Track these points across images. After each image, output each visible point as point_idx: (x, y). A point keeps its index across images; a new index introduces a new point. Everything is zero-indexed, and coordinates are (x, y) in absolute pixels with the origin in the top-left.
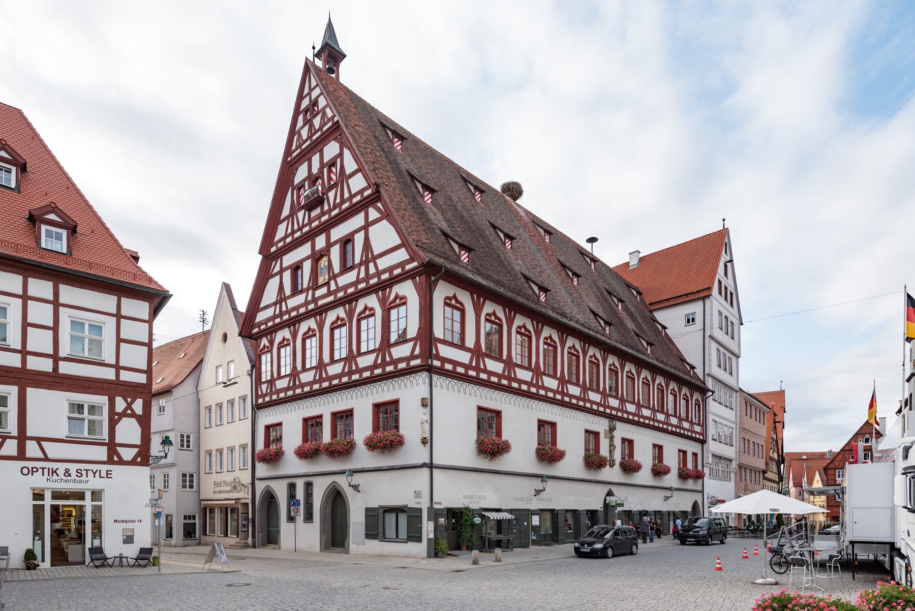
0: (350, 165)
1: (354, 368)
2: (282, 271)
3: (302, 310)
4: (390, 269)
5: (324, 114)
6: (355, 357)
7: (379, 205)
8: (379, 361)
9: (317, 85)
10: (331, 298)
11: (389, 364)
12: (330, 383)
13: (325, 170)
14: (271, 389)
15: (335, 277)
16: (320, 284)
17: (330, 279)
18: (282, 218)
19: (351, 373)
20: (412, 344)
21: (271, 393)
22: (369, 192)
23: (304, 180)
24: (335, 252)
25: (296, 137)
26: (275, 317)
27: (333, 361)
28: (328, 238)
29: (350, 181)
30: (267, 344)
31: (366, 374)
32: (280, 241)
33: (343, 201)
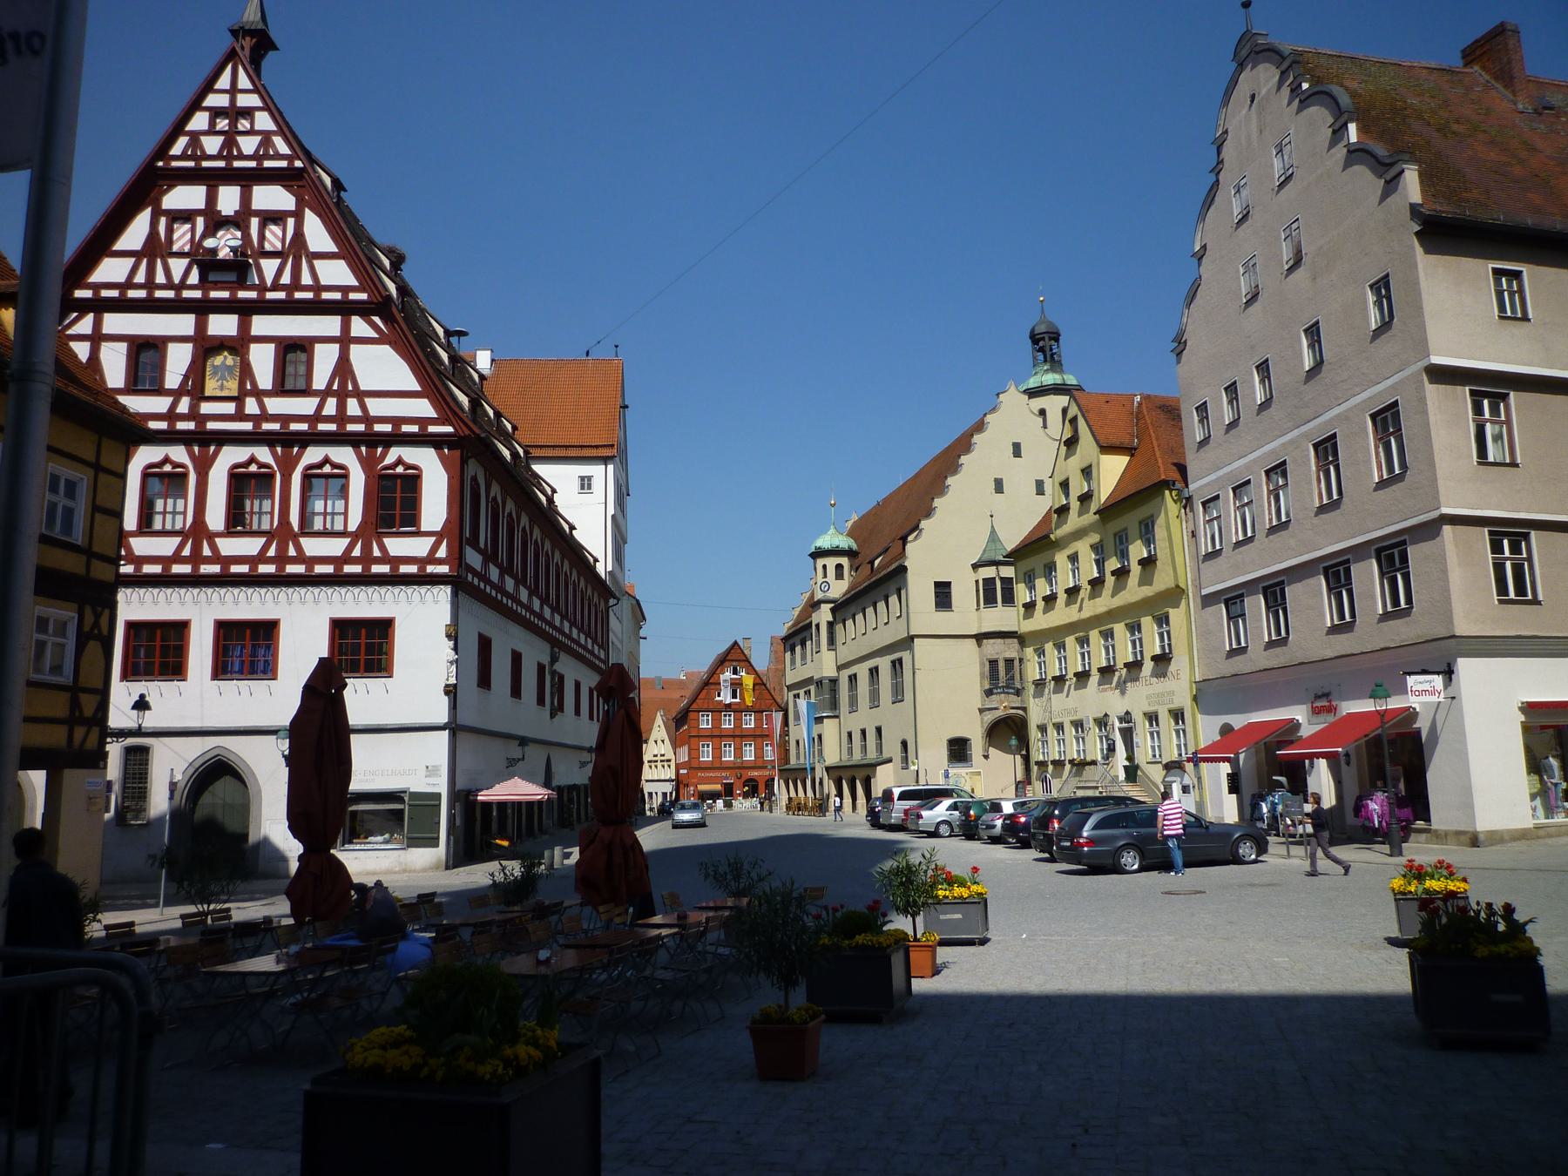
4: (397, 421)
7: (376, 319)
10: (247, 426)
13: (255, 222)
18: (118, 246)
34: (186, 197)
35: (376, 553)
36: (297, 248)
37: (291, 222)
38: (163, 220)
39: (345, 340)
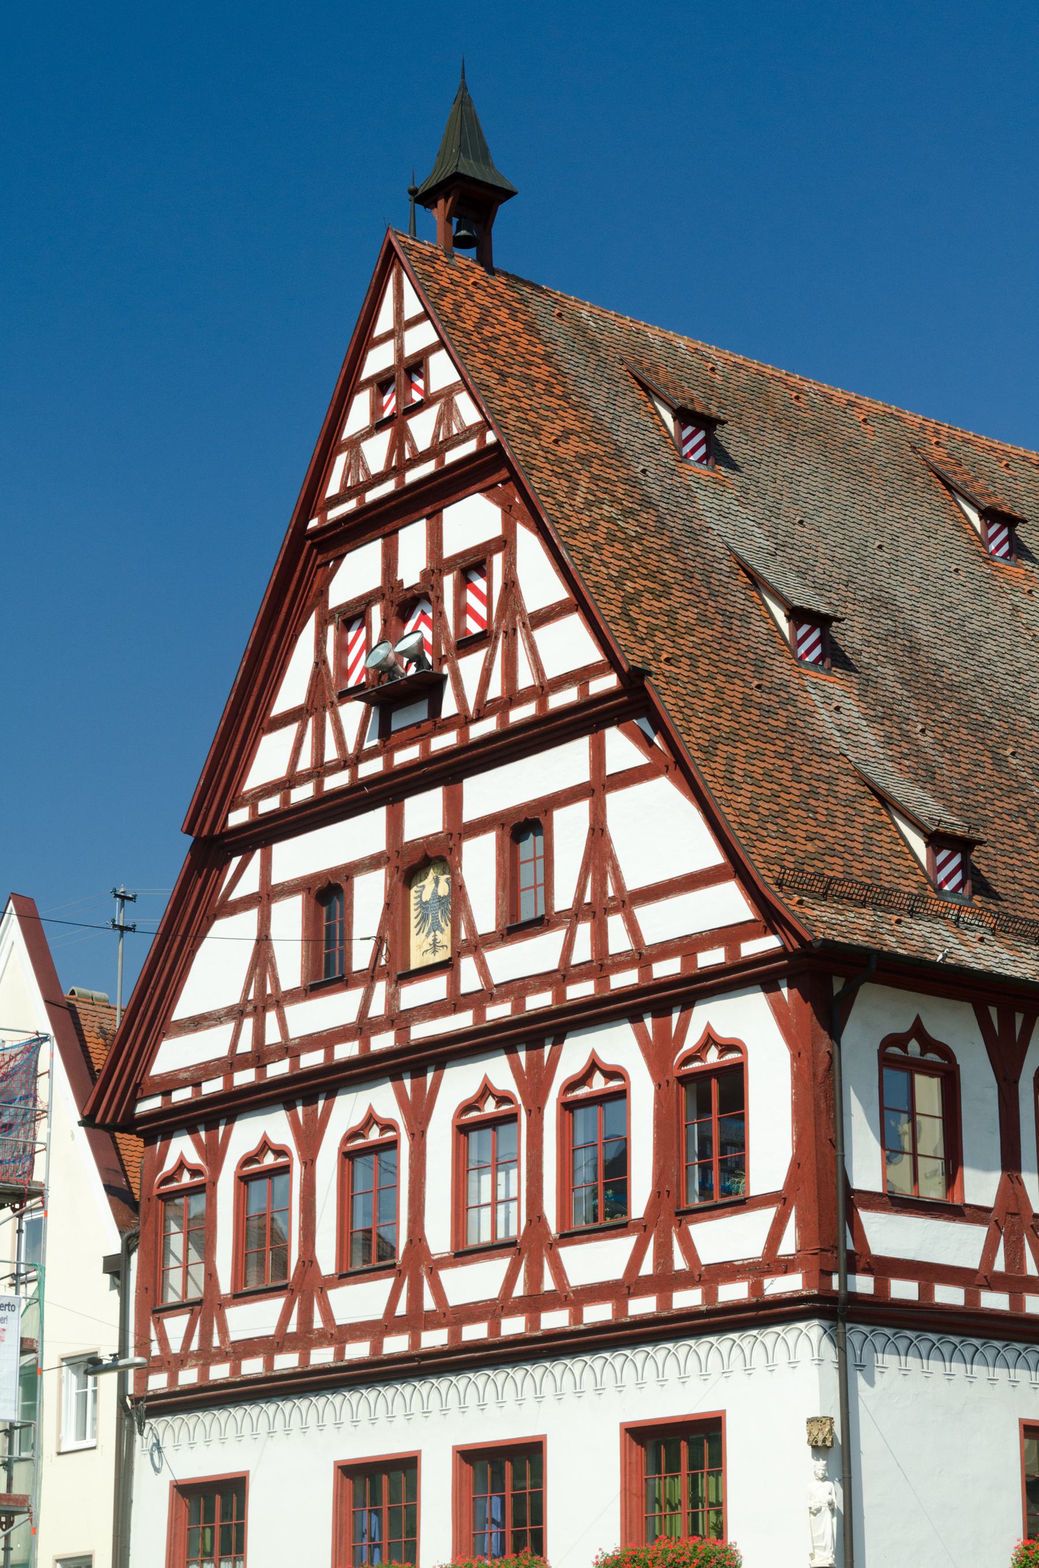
0: (540, 582)
1: (549, 1284)
2: (266, 896)
3: (347, 1051)
4: (687, 946)
5: (449, 412)
6: (553, 1247)
8: (647, 1268)
9: (425, 316)
10: (463, 1020)
11: (685, 1280)
12: (455, 1335)
13: (449, 582)
14: (206, 1337)
15: (477, 945)
16: (415, 964)
17: (458, 953)
19: (536, 1303)
20: (768, 1214)
21: (207, 1357)
22: (609, 682)
23: (366, 601)
24: (479, 858)
25: (341, 461)
26: (233, 1062)
27: (464, 1253)
28: (453, 806)
29: (540, 635)
30: (194, 1158)
31: (598, 1313)
32: (267, 790)
33: (512, 698)
34: (357, 574)
35: (680, 1263)
36: (513, 620)
37: (498, 560)
38: (331, 630)
39: (597, 788)
